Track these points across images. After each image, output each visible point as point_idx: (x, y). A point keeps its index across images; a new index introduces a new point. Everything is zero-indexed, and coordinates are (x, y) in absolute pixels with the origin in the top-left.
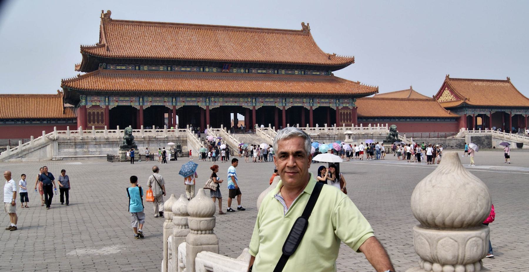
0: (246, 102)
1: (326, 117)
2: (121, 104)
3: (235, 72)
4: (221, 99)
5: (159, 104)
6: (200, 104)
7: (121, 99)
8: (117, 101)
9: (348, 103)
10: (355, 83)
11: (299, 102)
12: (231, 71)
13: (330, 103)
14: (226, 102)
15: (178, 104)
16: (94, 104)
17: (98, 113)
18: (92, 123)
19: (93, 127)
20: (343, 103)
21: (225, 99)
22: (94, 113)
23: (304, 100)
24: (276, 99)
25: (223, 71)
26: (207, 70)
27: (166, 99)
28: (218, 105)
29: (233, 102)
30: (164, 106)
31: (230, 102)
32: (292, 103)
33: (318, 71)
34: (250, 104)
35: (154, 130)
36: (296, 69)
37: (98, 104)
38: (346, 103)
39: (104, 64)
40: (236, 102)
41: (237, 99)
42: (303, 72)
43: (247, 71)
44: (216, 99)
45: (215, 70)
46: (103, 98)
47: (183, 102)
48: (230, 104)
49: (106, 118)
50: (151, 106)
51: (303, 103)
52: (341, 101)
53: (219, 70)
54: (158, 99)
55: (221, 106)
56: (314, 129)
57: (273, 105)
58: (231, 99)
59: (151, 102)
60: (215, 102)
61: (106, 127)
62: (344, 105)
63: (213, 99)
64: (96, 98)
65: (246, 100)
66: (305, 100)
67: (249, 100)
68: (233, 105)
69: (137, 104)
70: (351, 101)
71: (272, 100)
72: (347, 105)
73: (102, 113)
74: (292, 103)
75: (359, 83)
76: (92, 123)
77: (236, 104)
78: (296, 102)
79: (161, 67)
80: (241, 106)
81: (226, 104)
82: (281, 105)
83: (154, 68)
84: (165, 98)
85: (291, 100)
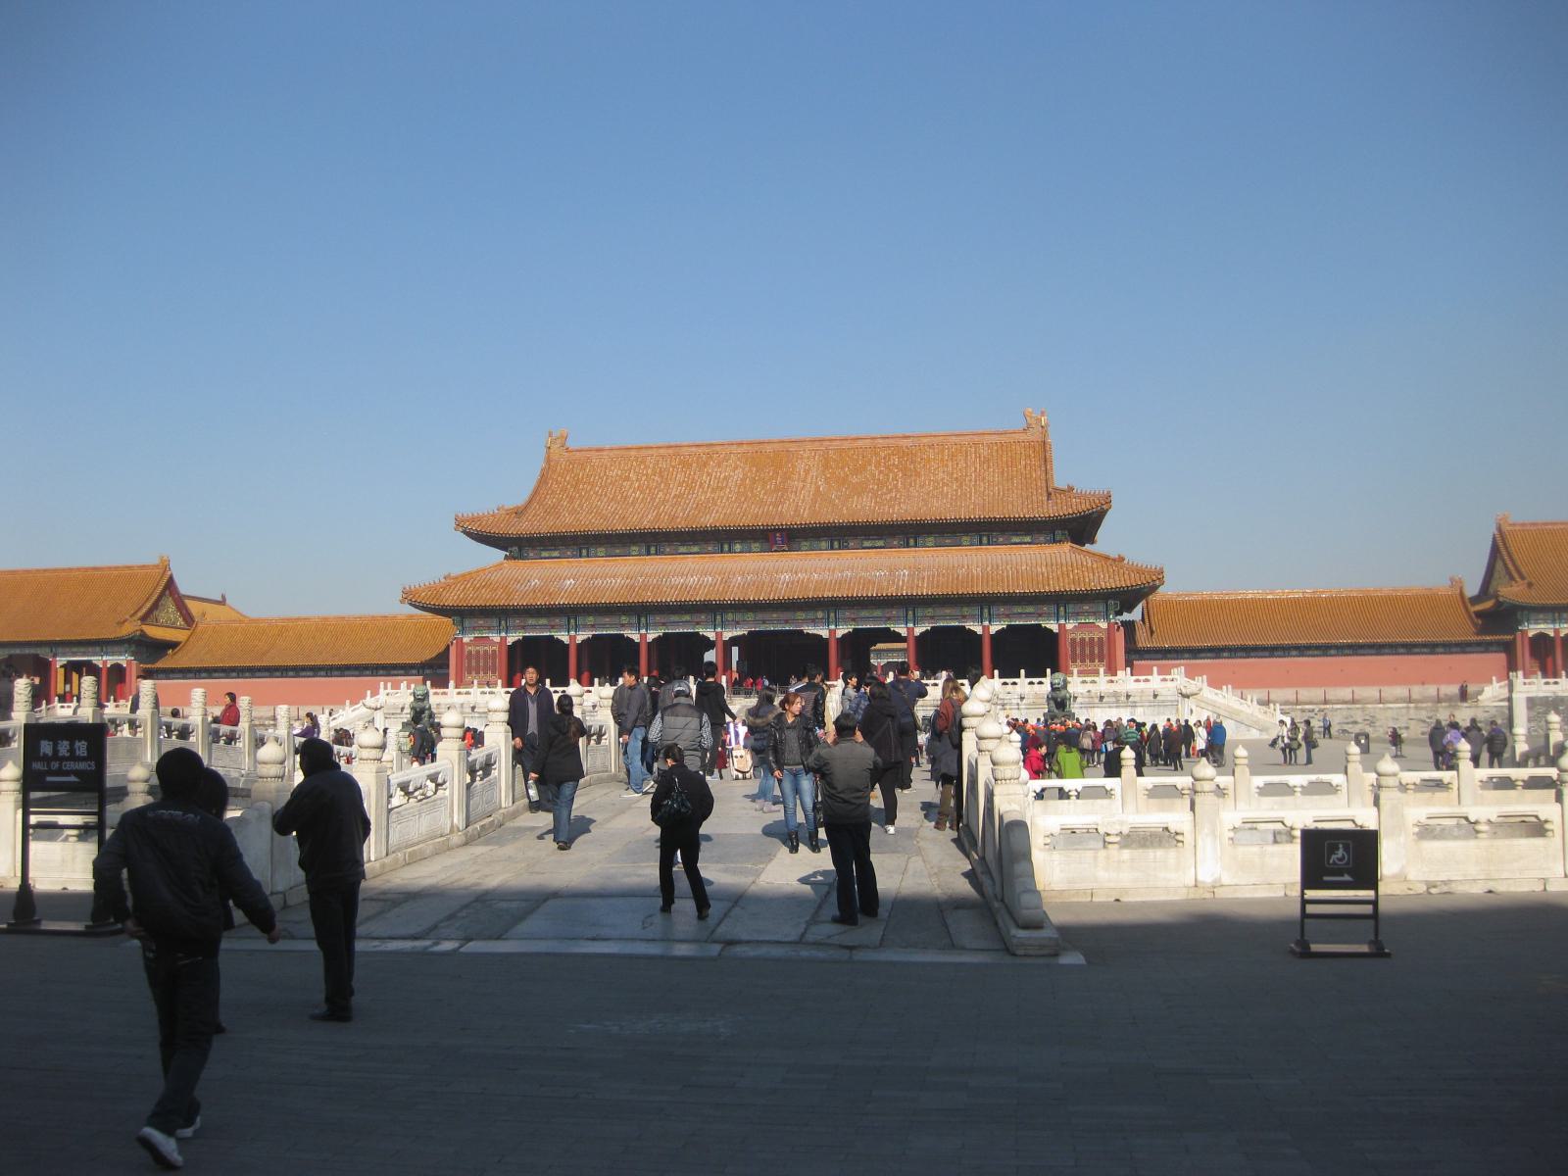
4: (750, 616)
7: (531, 621)
10: (1114, 560)
14: (764, 622)
17: (486, 652)
18: (474, 673)
21: (760, 616)
22: (478, 652)
24: (887, 610)
27: (624, 619)
29: (779, 621)
31: (771, 621)
35: (475, 690)
38: (1089, 614)
40: (787, 622)
41: (788, 615)
44: (739, 617)
49: (502, 662)
58: (775, 615)
61: (500, 681)
65: (811, 615)
67: (820, 614)
68: (779, 628)
73: (494, 651)
75: (1121, 559)
76: (474, 673)
84: (623, 618)
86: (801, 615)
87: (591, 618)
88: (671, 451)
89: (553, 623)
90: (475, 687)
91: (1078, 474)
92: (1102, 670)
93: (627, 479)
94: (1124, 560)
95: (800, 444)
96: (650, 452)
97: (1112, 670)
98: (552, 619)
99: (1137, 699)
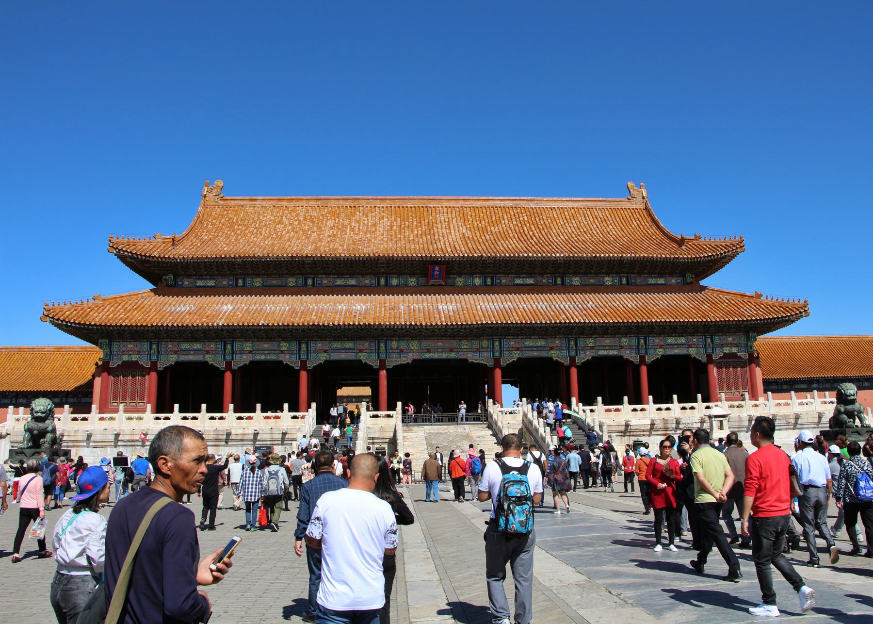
0: (478, 350)
1: (681, 380)
2: (184, 358)
3: (459, 284)
4: (414, 345)
5: (269, 357)
6: (363, 357)
7: (185, 346)
8: (176, 352)
9: (736, 345)
11: (611, 347)
12: (450, 282)
13: (690, 346)
14: (429, 351)
15: (312, 356)
16: (125, 358)
19: (122, 406)
20: (722, 346)
21: (425, 344)
23: (624, 340)
25: (431, 282)
26: (394, 281)
27: (284, 346)
28: (407, 359)
29: (444, 350)
30: (281, 362)
32: (592, 348)
33: (661, 275)
34: (485, 354)
36: (608, 274)
37: (134, 358)
38: (731, 345)
39: (171, 277)
40: (451, 351)
41: (454, 344)
42: (624, 280)
43: (489, 281)
44: (403, 345)
45: (412, 281)
46: (145, 346)
47: (325, 351)
48: (436, 356)
50: (251, 362)
51: (622, 347)
52: (717, 340)
53: (422, 281)
54: (266, 346)
55: (414, 361)
56: (642, 410)
57: (544, 354)
58: (440, 344)
59: (250, 352)
60: (402, 351)
62: (727, 350)
63: (394, 344)
64: (130, 346)
65: (476, 344)
66: (624, 341)
67: (485, 343)
68: (444, 356)
69: (219, 358)
70: (743, 340)
71: (541, 343)
72: (735, 350)
74: (592, 348)
75: (759, 296)
77: (453, 355)
78: (603, 348)
79: (291, 279)
80: (466, 360)
81: (427, 356)
82: (565, 353)
83: (274, 282)
84: (283, 344)
85: (591, 342)
86: (465, 344)
87: (249, 344)
88: (319, 203)
89: (207, 349)
90: (121, 412)
91: (696, 225)
92: (747, 395)
93: (281, 223)
94: (761, 295)
95: (438, 202)
96: (300, 203)
97: (754, 396)
98: (207, 343)
99: (804, 421)
